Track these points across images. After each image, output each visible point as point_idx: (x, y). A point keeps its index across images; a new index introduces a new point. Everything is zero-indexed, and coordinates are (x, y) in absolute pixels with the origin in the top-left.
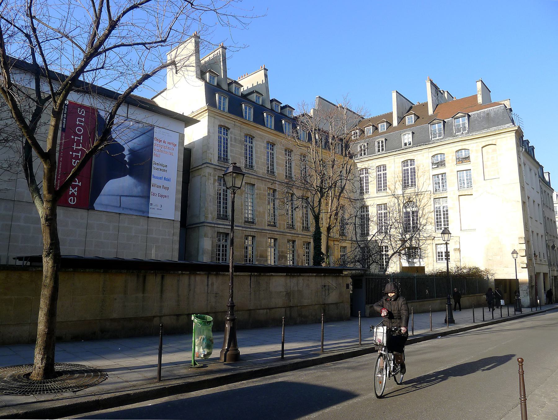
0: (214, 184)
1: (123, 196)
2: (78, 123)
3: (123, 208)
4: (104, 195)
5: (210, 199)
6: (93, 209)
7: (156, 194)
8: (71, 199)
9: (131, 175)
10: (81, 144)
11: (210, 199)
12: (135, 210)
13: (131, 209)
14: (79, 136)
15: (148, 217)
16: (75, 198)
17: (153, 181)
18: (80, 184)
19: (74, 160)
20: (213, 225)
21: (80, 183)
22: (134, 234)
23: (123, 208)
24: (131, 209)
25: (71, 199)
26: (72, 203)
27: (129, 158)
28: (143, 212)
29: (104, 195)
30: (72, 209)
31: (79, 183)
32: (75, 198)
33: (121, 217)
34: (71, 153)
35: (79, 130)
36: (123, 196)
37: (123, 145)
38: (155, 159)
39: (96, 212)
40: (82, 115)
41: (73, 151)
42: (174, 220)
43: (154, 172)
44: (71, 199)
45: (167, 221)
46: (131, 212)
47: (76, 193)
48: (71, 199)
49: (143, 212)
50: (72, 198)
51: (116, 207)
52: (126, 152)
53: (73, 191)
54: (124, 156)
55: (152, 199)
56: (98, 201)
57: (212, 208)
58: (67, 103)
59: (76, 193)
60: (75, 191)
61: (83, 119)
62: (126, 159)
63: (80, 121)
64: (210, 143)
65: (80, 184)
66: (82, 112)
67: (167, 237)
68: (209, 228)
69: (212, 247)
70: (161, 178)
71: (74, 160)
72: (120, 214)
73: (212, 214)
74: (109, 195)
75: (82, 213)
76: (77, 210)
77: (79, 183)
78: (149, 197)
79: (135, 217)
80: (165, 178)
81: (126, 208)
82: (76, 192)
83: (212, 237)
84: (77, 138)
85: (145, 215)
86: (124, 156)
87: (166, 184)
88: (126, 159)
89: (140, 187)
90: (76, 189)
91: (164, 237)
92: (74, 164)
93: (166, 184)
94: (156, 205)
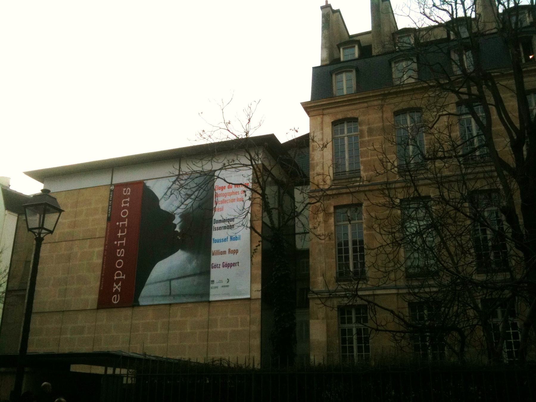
0: (326, 222)
1: (174, 279)
2: (123, 205)
3: (174, 296)
4: (151, 284)
6: (139, 305)
7: (218, 266)
8: (115, 297)
9: (183, 249)
10: (126, 229)
11: (320, 250)
13: (184, 295)
14: (124, 220)
15: (210, 302)
16: (119, 295)
17: (215, 247)
18: (124, 277)
21: (125, 275)
22: (189, 331)
23: (174, 296)
24: (184, 295)
25: (114, 298)
26: (115, 302)
27: (181, 228)
28: (202, 295)
29: (151, 284)
30: (115, 310)
31: (123, 276)
32: (119, 295)
34: (116, 243)
36: (174, 279)
38: (217, 216)
39: (142, 308)
40: (128, 194)
41: (118, 239)
43: (216, 235)
44: (115, 297)
45: (239, 302)
46: (185, 300)
47: (119, 289)
48: (114, 298)
49: (202, 295)
50: (116, 296)
52: (177, 220)
53: (117, 287)
54: (175, 226)
55: (215, 274)
56: (145, 291)
57: (324, 265)
59: (119, 289)
60: (119, 287)
61: (128, 200)
62: (177, 229)
64: (315, 157)
65: (124, 277)
66: (127, 192)
67: (240, 328)
69: (328, 336)
70: (225, 240)
71: (118, 250)
72: (170, 304)
74: (156, 283)
75: (127, 312)
76: (122, 309)
77: (123, 276)
78: (208, 273)
79: (190, 305)
81: (179, 295)
84: (126, 224)
85: (204, 299)
86: (175, 226)
88: (177, 229)
90: (120, 284)
94: (221, 281)
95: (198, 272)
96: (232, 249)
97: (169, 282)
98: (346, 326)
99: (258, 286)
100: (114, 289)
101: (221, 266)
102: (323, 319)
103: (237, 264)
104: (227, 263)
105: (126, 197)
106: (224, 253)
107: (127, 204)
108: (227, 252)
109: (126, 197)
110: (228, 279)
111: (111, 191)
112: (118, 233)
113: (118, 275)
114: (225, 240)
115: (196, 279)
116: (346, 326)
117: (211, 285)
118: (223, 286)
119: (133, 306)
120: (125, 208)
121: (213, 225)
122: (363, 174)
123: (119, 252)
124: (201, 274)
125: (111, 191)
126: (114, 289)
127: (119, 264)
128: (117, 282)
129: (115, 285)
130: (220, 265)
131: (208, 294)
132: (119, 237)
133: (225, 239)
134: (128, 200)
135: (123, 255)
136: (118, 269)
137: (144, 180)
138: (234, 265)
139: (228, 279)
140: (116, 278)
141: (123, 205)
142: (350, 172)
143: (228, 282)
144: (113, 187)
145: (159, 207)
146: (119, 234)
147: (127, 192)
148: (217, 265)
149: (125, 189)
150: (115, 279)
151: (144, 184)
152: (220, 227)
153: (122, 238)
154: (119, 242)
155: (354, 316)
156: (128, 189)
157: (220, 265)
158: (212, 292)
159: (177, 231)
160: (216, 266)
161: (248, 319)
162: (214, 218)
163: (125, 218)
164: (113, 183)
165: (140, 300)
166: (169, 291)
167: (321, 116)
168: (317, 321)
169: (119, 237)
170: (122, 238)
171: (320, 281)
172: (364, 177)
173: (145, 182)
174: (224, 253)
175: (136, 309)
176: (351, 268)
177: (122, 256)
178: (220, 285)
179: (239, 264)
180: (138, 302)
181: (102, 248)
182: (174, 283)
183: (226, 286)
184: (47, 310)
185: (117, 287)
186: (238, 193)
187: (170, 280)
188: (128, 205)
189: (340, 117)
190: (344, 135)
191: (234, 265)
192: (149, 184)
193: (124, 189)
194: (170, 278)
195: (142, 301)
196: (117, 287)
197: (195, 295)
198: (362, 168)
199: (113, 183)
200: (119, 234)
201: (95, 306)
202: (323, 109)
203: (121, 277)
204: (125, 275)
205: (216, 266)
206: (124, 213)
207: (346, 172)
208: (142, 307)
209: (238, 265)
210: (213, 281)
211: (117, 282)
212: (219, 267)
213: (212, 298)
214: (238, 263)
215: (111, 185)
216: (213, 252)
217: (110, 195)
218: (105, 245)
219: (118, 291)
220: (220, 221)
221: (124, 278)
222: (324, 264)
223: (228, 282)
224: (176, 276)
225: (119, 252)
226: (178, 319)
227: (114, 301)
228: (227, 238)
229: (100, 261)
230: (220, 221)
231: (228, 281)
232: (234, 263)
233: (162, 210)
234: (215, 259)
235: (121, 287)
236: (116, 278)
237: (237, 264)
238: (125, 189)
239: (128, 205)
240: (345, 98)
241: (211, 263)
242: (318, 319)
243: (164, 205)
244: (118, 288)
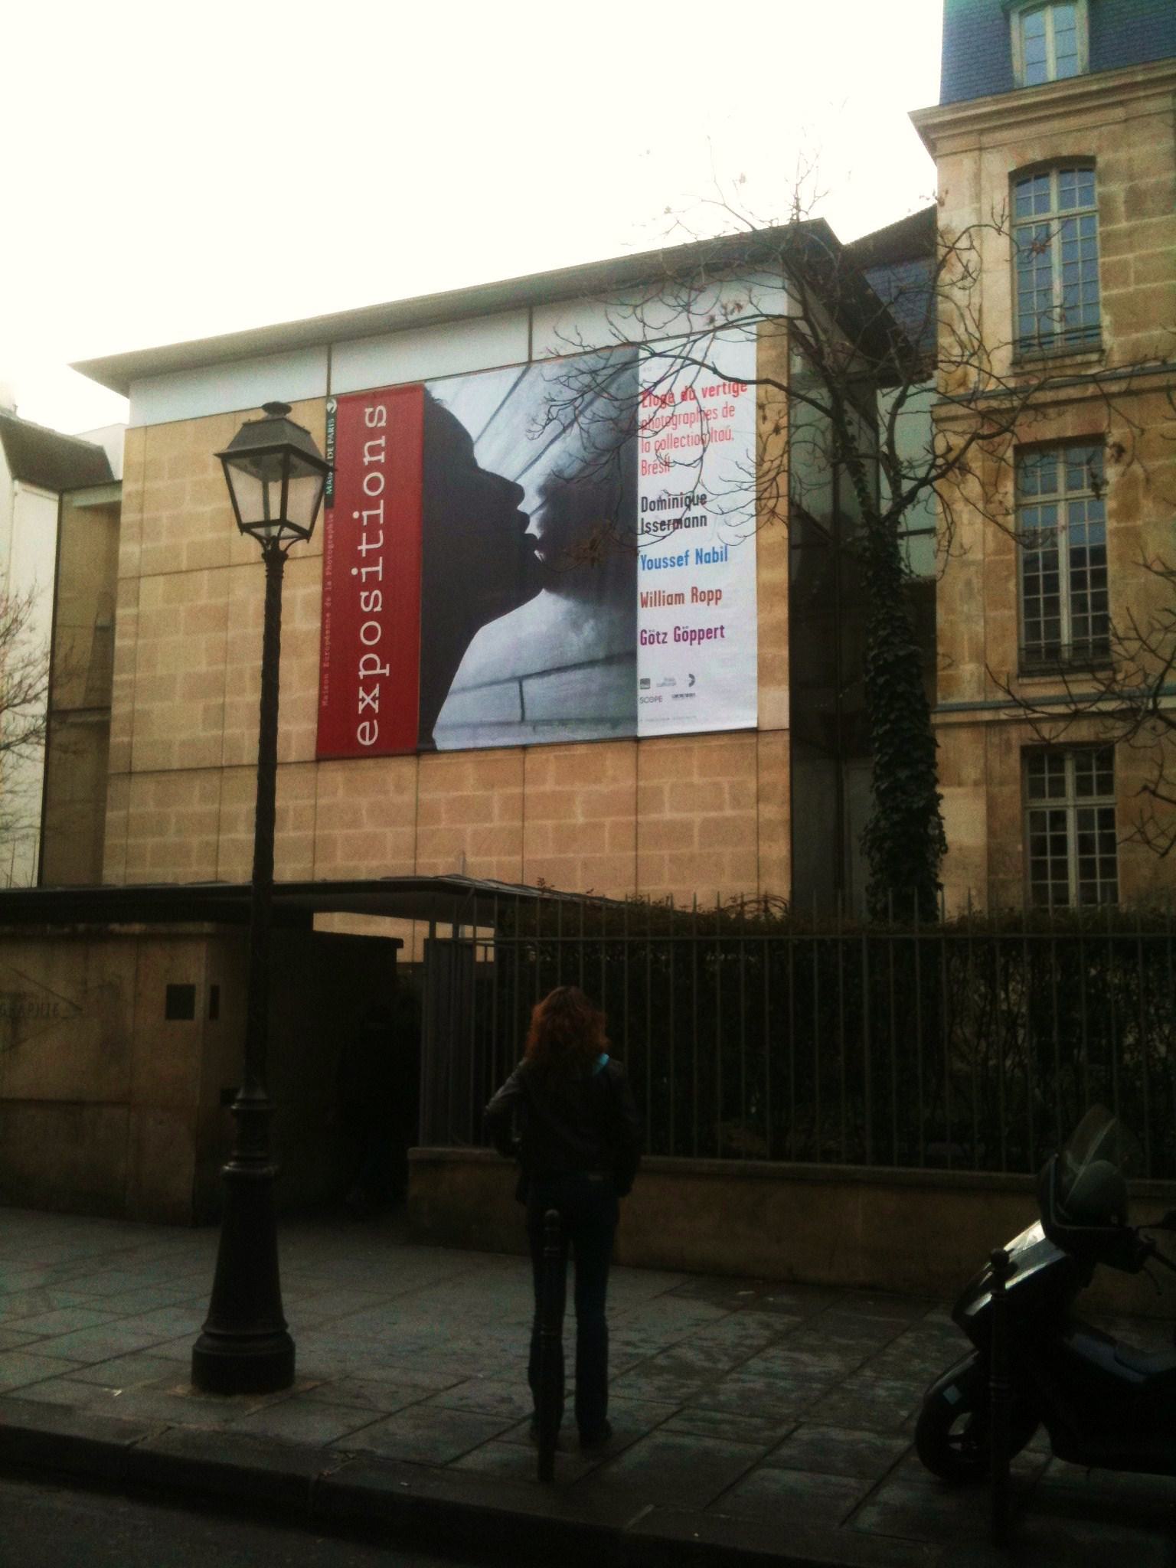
1: (529, 676)
2: (367, 459)
3: (536, 724)
4: (464, 690)
5: (968, 583)
6: (433, 751)
7: (661, 637)
8: (364, 728)
9: (554, 587)
10: (381, 532)
11: (968, 583)
12: (581, 721)
13: (563, 722)
14: (372, 503)
15: (638, 740)
16: (375, 722)
17: (647, 581)
18: (387, 671)
19: (364, 594)
20: (987, 716)
21: (388, 666)
22: (581, 820)
23: (536, 724)
25: (364, 730)
26: (367, 743)
27: (544, 524)
28: (615, 723)
29: (464, 690)
30: (369, 763)
31: (383, 667)
32: (375, 722)
33: (533, 758)
34: (354, 571)
35: (374, 484)
36: (529, 676)
37: (518, 478)
38: (648, 486)
39: (444, 759)
40: (379, 425)
42: (755, 731)
43: (648, 547)
44: (364, 728)
45: (725, 741)
46: (564, 735)
47: (376, 706)
48: (364, 730)
49: (615, 723)
50: (367, 724)
51: (508, 724)
52: (531, 504)
53: (368, 700)
54: (525, 519)
55: (650, 661)
56: (452, 710)
57: (979, 628)
58: (332, 409)
59: (376, 706)
60: (374, 699)
61: (382, 442)
62: (533, 529)
63: (373, 451)
65: (387, 671)
66: (377, 417)
67: (729, 812)
68: (965, 735)
69: (991, 833)
70: (680, 561)
71: (364, 594)
72: (524, 748)
73: (980, 656)
74: (479, 686)
75: (403, 769)
77: (383, 667)
78: (631, 657)
79: (581, 750)
80: (699, 555)
81: (548, 722)
82: (377, 702)
83: (987, 778)
84: (382, 516)
85: (620, 732)
86: (525, 519)
87: (706, 577)
88: (533, 529)
89: (592, 622)
90: (376, 692)
91: (713, 814)
92: (367, 604)
93: (706, 577)
94: (671, 682)
95: (601, 654)
96: (703, 587)
97: (516, 686)
98: (1048, 804)
99: (780, 696)
100: (361, 706)
101: (670, 637)
102: (976, 784)
103: (719, 632)
104: (688, 630)
105: (373, 434)
106: (679, 598)
107: (379, 454)
108: (688, 597)
109: (373, 434)
110: (691, 676)
111: (329, 415)
112: (361, 544)
113: (371, 664)
114: (680, 561)
115: (598, 675)
116: (1048, 804)
117: (642, 693)
118: (676, 696)
119: (418, 753)
120: (374, 466)
121: (640, 515)
122: (1108, 339)
123: (367, 599)
124: (609, 660)
125: (329, 415)
126: (361, 706)
127: (370, 634)
128: (368, 684)
129: (362, 694)
130: (665, 634)
131: (633, 719)
132: (364, 555)
133: (680, 558)
134: (382, 442)
135: (378, 609)
136: (371, 649)
137: (426, 380)
138: (709, 634)
139: (691, 676)
140: (362, 673)
141: (367, 459)
142: (1068, 336)
143: (691, 684)
144: (332, 406)
145: (472, 463)
146: (364, 547)
147: (377, 417)
148: (658, 634)
149: (371, 410)
150: (362, 677)
151: (427, 394)
152: (663, 523)
153: (371, 558)
154: (364, 570)
155: (1070, 775)
156: (377, 411)
157: (665, 634)
158: (644, 711)
159: (532, 536)
160: (654, 638)
161: (752, 786)
162: (641, 493)
163: (378, 497)
164: (333, 392)
165: (436, 735)
166: (519, 712)
167: (976, 153)
168: (960, 790)
169: (364, 555)
170: (371, 558)
171: (967, 676)
172: (1111, 349)
173: (428, 385)
174: (679, 598)
175: (428, 762)
176: (1066, 636)
177: (376, 610)
178: (667, 692)
179: (724, 631)
180: (432, 741)
181: (317, 589)
182: (532, 687)
183: (687, 695)
184: (176, 765)
185: (367, 700)
186: (714, 415)
187: (520, 680)
188: (382, 457)
189: (1036, 155)
190: (1048, 215)
191: (709, 634)
192: (440, 392)
193: (369, 410)
194: (520, 673)
195: (443, 740)
196: (367, 700)
197: (599, 721)
198: (1106, 320)
199: (333, 392)
200: (364, 547)
201: (310, 753)
202: (982, 132)
203: (378, 671)
204: (388, 666)
205: (654, 638)
206: (374, 484)
207: (1053, 334)
208: (445, 756)
209: (722, 636)
210: (646, 682)
211: (368, 684)
212: (664, 642)
213: (643, 730)
214: (722, 628)
215: (328, 397)
216: (645, 595)
217: (327, 428)
218: (325, 579)
219: (374, 709)
220: (660, 503)
221: (388, 674)
222: (982, 623)
223: (691, 684)
224: (538, 668)
225: (367, 599)
226: (549, 787)
227: (364, 738)
228: (687, 556)
229: (316, 625)
230: (660, 503)
231: (690, 679)
232: (709, 631)
233: (483, 472)
234: (648, 619)
235: (381, 698)
236: (362, 673)
237: (719, 632)
238: (371, 410)
239: (382, 457)
240: (1054, 90)
241: (639, 630)
242: (960, 784)
243: (488, 457)
244: (371, 703)
